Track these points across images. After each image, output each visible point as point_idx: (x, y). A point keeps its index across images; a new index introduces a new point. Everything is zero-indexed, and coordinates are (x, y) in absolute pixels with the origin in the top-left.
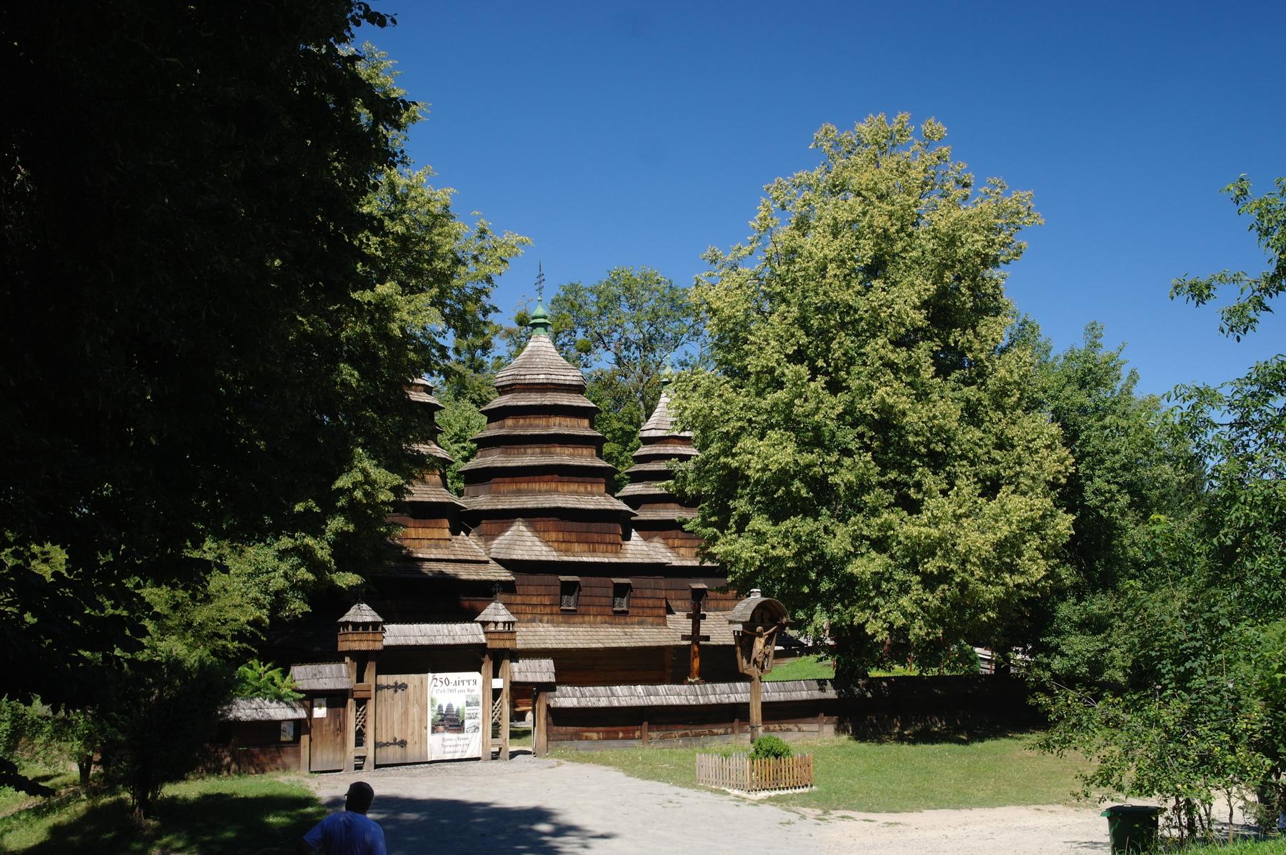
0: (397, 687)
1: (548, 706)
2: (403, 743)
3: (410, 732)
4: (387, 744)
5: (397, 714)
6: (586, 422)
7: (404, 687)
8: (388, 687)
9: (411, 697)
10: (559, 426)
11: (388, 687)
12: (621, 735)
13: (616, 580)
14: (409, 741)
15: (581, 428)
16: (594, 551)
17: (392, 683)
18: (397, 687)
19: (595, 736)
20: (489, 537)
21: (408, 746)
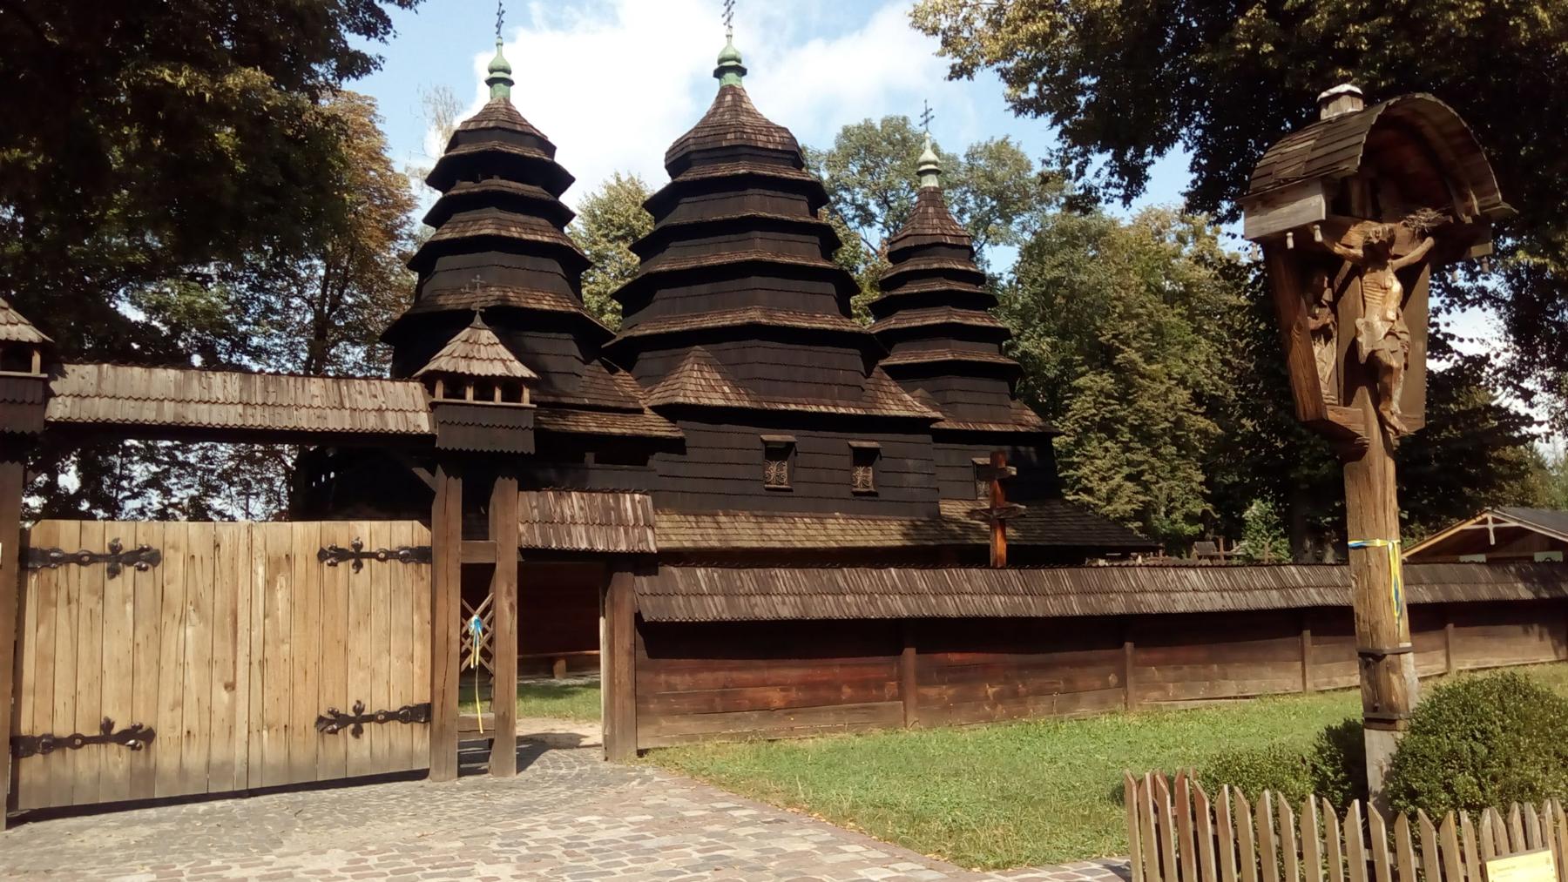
0: (116, 560)
1: (638, 617)
2: (141, 736)
3: (168, 696)
4: (75, 742)
5: (115, 646)
6: (804, 206)
7: (147, 558)
8: (82, 559)
9: (174, 591)
10: (756, 205)
11: (82, 559)
12: (847, 691)
13: (855, 444)
14: (163, 732)
15: (797, 211)
16: (821, 396)
17: (96, 545)
18: (116, 560)
19: (776, 697)
20: (649, 380)
21: (158, 744)
